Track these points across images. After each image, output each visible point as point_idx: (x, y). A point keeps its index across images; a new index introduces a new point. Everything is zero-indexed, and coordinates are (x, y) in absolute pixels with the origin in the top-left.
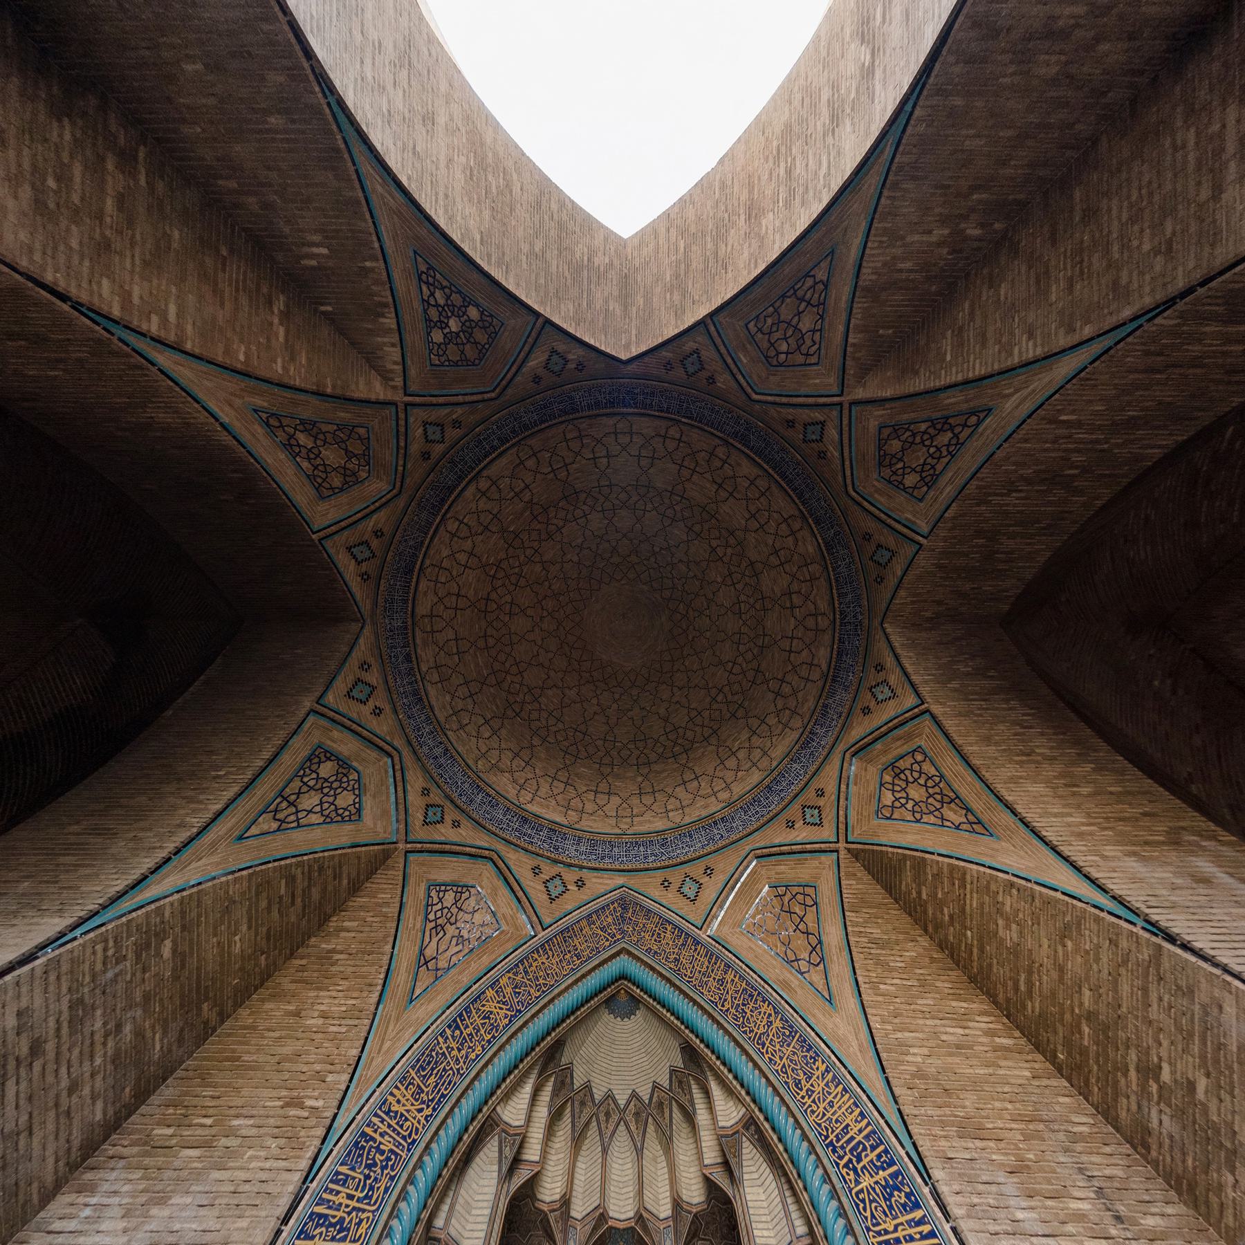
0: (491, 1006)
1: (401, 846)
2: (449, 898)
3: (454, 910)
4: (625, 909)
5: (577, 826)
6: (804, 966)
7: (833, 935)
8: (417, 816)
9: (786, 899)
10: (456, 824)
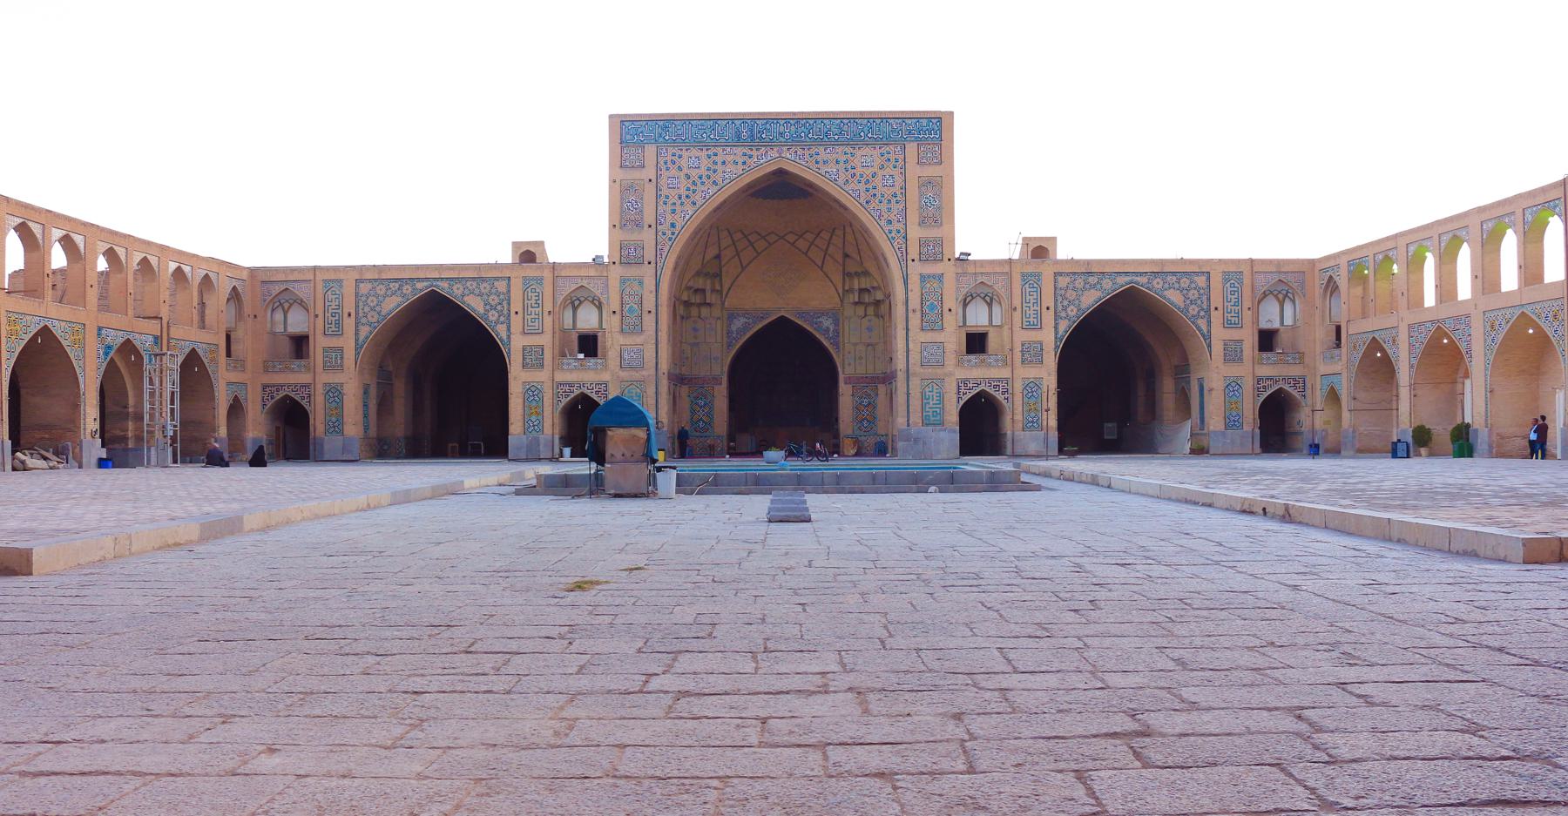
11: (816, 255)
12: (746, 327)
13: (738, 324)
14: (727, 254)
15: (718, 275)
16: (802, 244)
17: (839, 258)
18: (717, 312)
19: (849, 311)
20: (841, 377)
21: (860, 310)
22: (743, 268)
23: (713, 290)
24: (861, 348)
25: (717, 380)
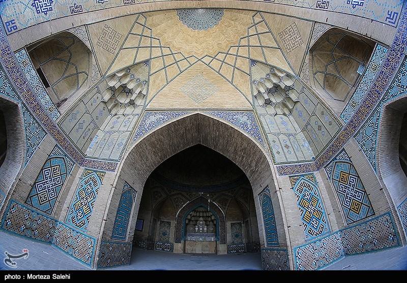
8: (168, 193)
11: (227, 71)
12: (158, 121)
14: (156, 65)
15: (147, 82)
16: (215, 64)
18: (138, 111)
19: (260, 111)
20: (273, 168)
21: (271, 110)
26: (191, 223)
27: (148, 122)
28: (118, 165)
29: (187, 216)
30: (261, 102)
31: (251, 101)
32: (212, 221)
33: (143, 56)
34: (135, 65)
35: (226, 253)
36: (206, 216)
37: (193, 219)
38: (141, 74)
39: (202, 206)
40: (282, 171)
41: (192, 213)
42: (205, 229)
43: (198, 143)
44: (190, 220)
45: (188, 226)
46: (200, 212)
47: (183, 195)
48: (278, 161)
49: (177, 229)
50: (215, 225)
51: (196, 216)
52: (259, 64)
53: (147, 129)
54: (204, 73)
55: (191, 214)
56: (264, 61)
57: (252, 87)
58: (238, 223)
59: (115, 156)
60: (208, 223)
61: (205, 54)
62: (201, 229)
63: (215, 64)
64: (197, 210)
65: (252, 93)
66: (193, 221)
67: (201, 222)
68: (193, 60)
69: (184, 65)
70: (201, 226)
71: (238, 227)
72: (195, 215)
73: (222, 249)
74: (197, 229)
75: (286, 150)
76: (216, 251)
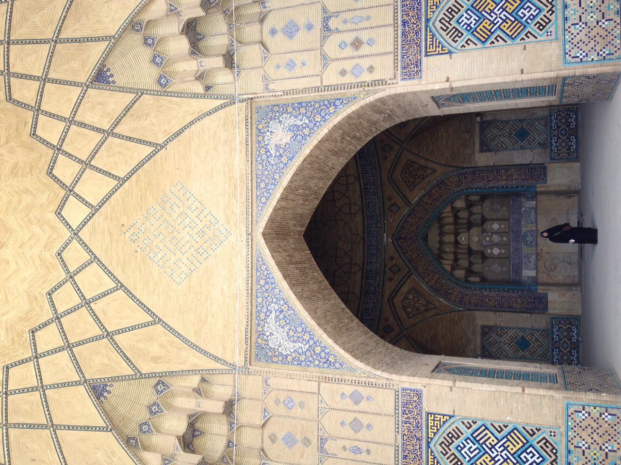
0: (434, 281)
1: (405, 333)
2: (409, 310)
3: (411, 307)
4: (401, 238)
5: (361, 265)
6: (425, 174)
7: (422, 162)
9: (407, 171)
10: (386, 320)
11: (119, 157)
12: (287, 319)
13: (278, 338)
14: (101, 362)
15: (161, 383)
16: (93, 187)
17: (116, 102)
18: (251, 385)
19: (250, 83)
20: (403, 87)
21: (249, 55)
22: (157, 320)
23: (198, 391)
24: (332, 47)
25: (410, 402)
26: (477, 268)
27: (288, 347)
28: (407, 386)
29: (458, 279)
30: (223, 78)
31: (219, 102)
32: (470, 205)
33: (80, 406)
34: (113, 425)
35: (576, 165)
36: (455, 223)
37: (464, 263)
38: (132, 402)
39: (426, 238)
40: (412, 69)
41: (447, 265)
42: (496, 226)
43: (302, 237)
44: (470, 272)
45: (489, 276)
46: (441, 242)
47: (395, 293)
48: (388, 74)
49: (498, 308)
50: (483, 198)
51: (455, 253)
52: (111, 59)
53: (311, 342)
54: (124, 220)
55: (448, 268)
56: (103, 45)
57: (180, 95)
58: (482, 131)
59: (386, 401)
60: (477, 218)
61: (52, 216)
62: (496, 238)
63: (93, 187)
64: (437, 252)
65: (196, 96)
66: (471, 264)
67: (472, 238)
68: (75, 255)
69: (93, 281)
70: (490, 239)
71: (496, 131)
72: (451, 256)
73: (560, 176)
74: (496, 251)
75: (365, 50)
76: (568, 193)
